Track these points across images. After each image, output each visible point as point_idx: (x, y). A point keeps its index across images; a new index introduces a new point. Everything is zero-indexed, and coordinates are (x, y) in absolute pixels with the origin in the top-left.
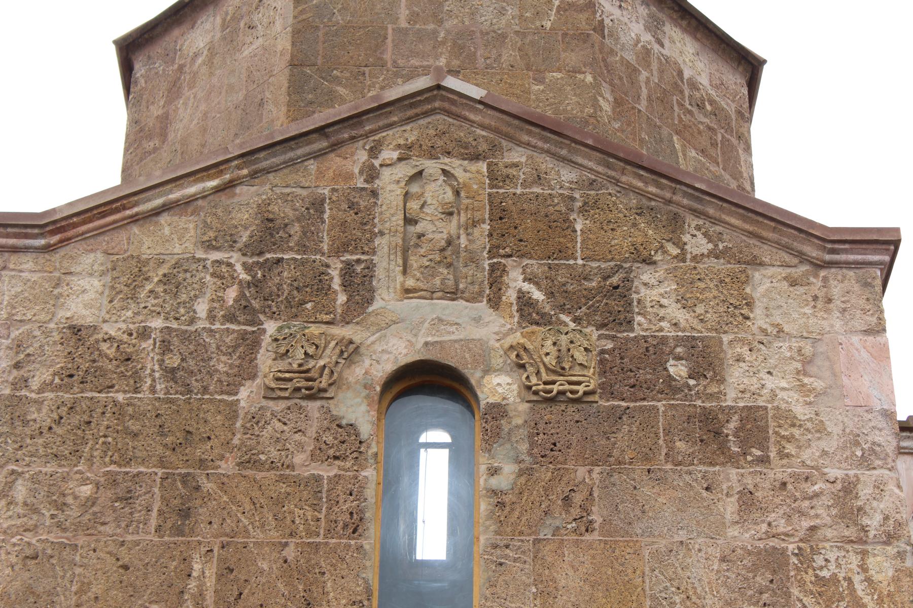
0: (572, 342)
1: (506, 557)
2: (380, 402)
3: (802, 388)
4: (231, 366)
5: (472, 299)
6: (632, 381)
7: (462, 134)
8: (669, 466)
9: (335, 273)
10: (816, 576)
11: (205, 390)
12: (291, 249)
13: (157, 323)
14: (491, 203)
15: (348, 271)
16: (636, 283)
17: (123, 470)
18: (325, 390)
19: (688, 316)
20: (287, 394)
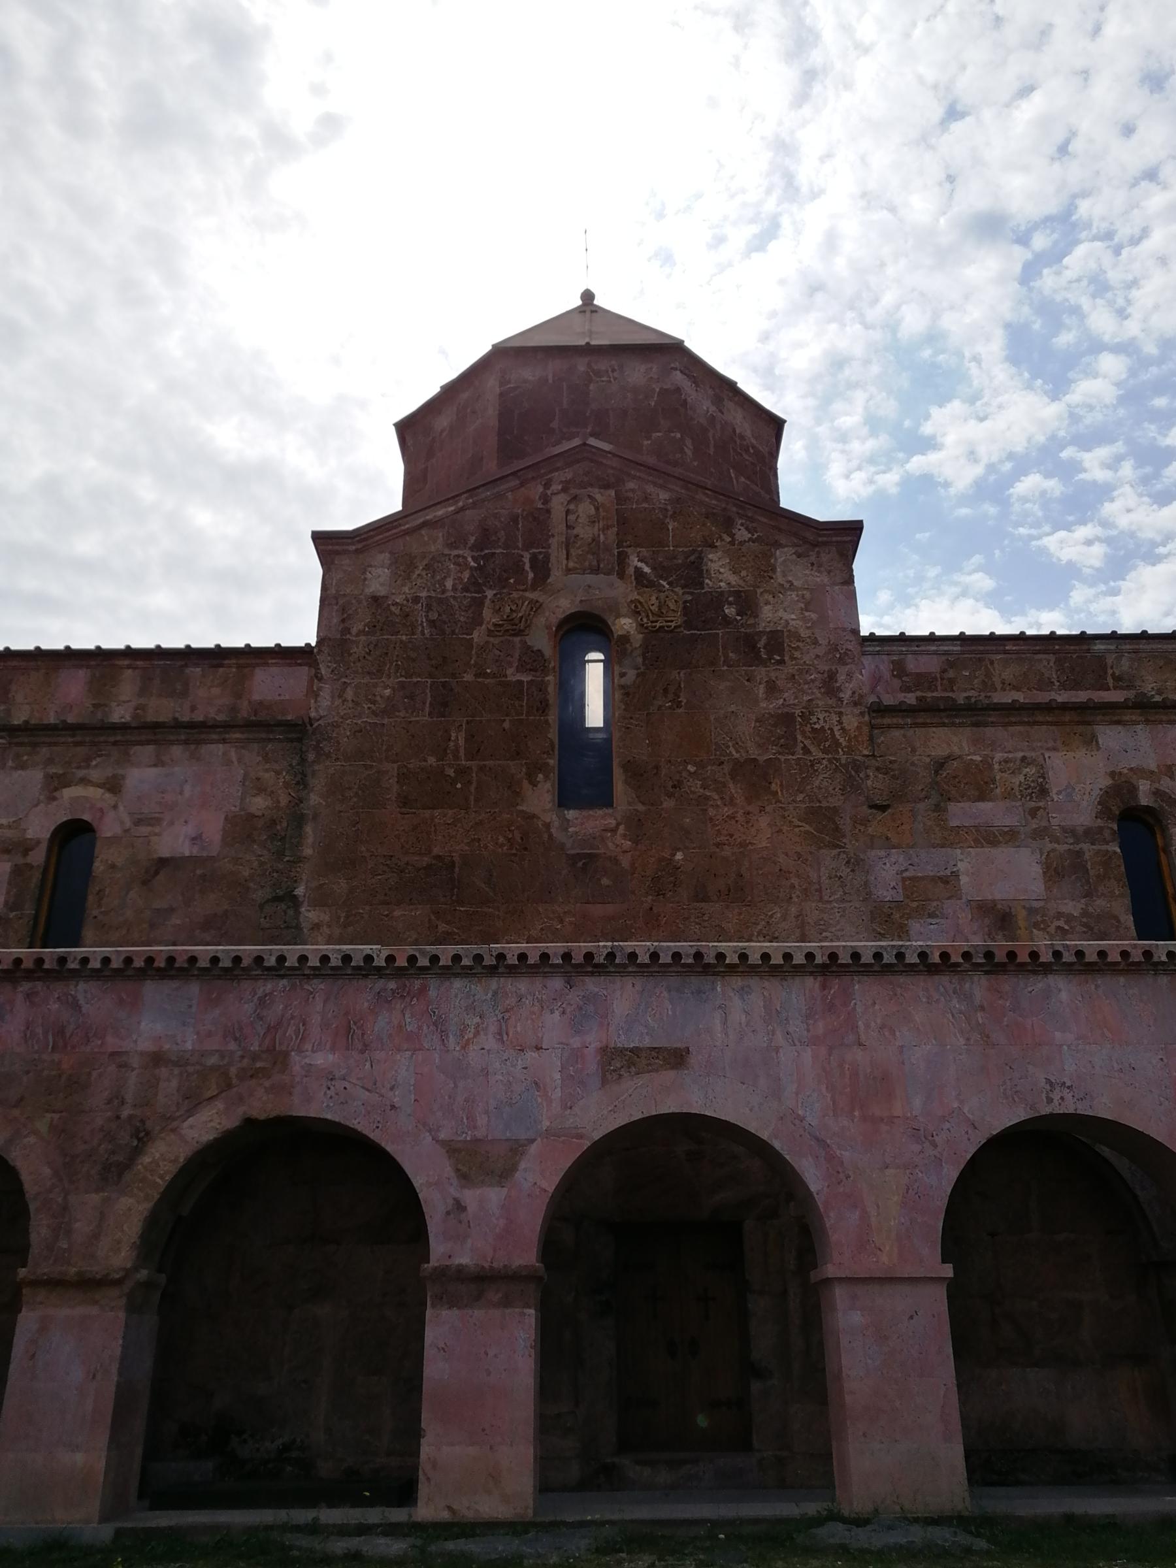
0: (667, 597)
1: (631, 724)
2: (555, 636)
3: (804, 619)
4: (468, 617)
5: (608, 574)
6: (703, 619)
7: (599, 473)
8: (725, 668)
9: (526, 560)
10: (812, 728)
11: (453, 632)
12: (500, 547)
13: (424, 594)
14: (617, 513)
15: (534, 559)
16: (705, 560)
17: (408, 680)
18: (523, 631)
19: (736, 578)
20: (501, 634)
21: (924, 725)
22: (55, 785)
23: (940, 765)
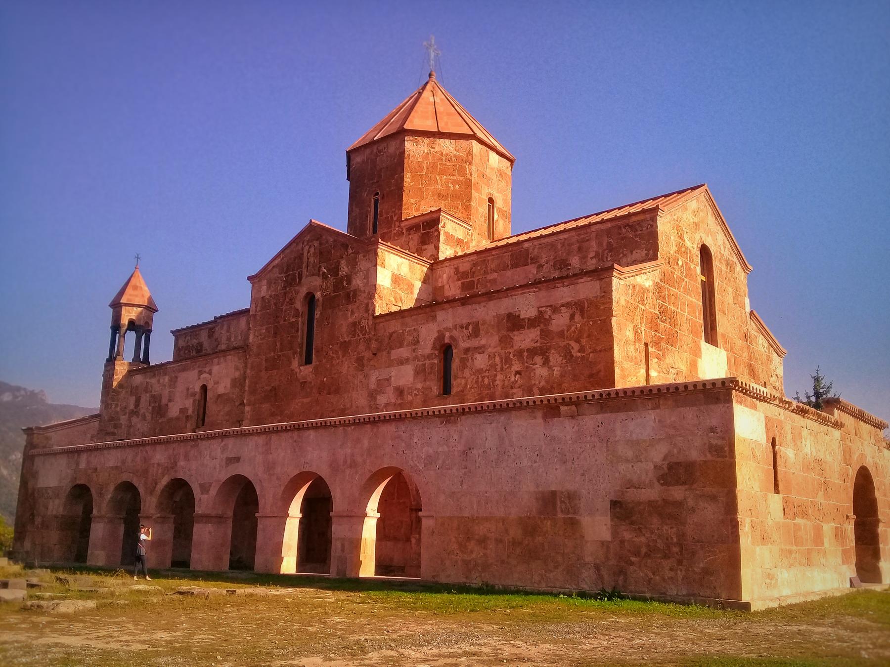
15: (299, 273)
21: (389, 320)
22: (200, 373)
23: (391, 335)
